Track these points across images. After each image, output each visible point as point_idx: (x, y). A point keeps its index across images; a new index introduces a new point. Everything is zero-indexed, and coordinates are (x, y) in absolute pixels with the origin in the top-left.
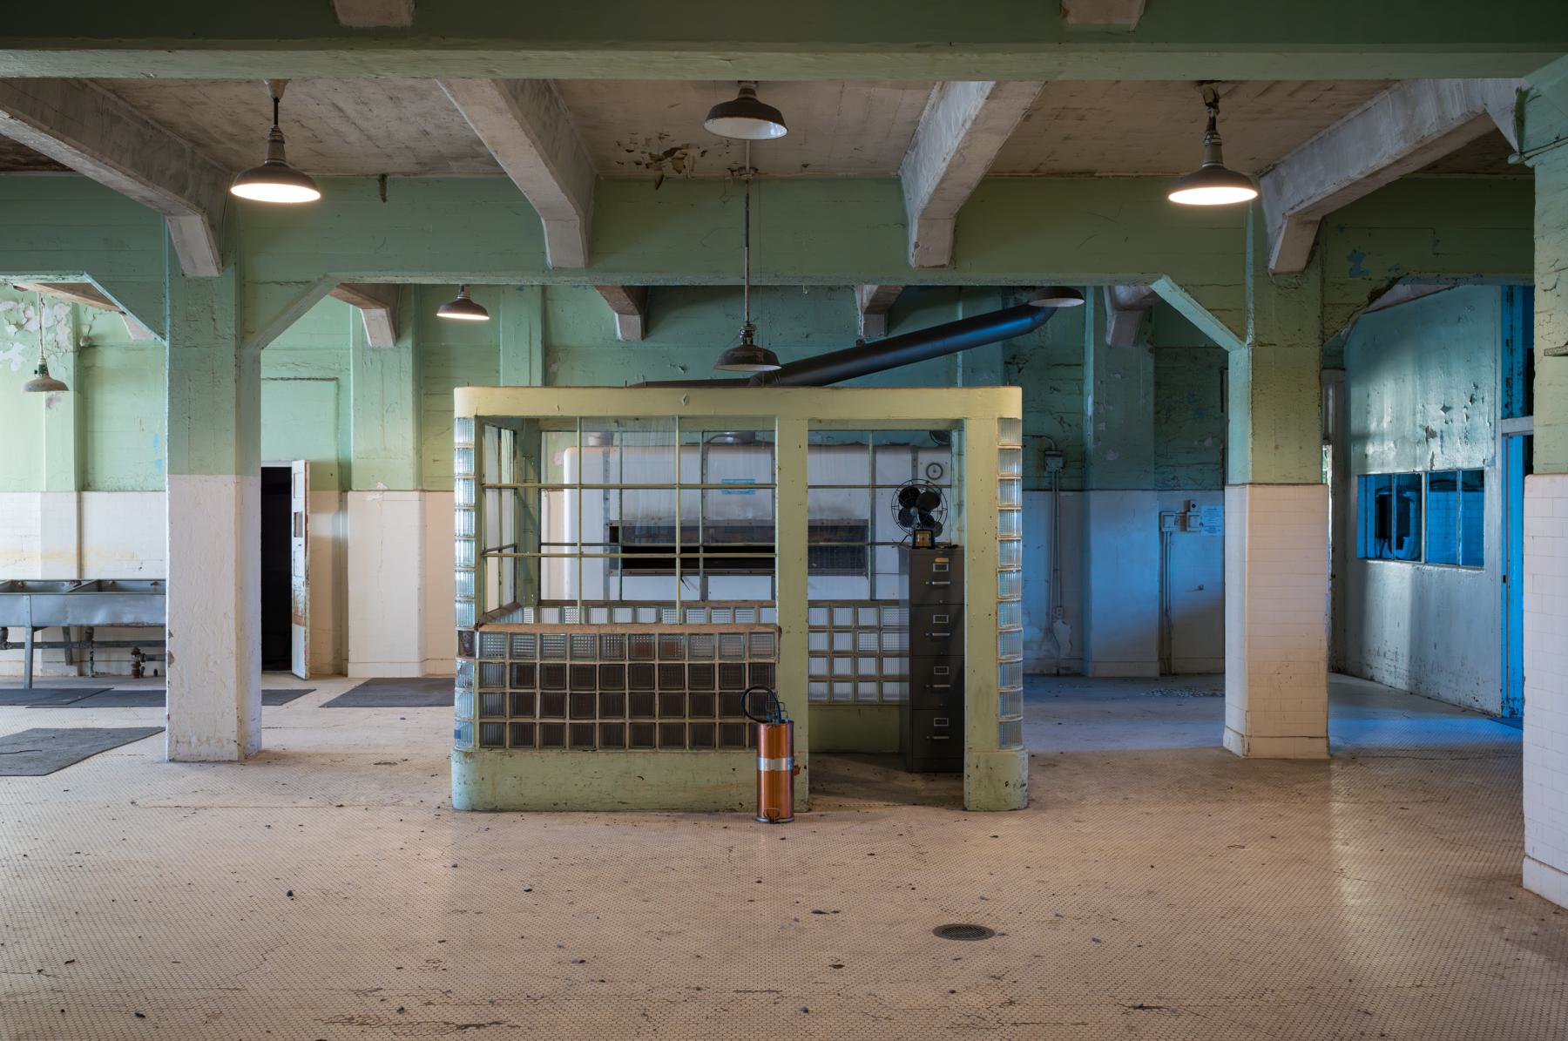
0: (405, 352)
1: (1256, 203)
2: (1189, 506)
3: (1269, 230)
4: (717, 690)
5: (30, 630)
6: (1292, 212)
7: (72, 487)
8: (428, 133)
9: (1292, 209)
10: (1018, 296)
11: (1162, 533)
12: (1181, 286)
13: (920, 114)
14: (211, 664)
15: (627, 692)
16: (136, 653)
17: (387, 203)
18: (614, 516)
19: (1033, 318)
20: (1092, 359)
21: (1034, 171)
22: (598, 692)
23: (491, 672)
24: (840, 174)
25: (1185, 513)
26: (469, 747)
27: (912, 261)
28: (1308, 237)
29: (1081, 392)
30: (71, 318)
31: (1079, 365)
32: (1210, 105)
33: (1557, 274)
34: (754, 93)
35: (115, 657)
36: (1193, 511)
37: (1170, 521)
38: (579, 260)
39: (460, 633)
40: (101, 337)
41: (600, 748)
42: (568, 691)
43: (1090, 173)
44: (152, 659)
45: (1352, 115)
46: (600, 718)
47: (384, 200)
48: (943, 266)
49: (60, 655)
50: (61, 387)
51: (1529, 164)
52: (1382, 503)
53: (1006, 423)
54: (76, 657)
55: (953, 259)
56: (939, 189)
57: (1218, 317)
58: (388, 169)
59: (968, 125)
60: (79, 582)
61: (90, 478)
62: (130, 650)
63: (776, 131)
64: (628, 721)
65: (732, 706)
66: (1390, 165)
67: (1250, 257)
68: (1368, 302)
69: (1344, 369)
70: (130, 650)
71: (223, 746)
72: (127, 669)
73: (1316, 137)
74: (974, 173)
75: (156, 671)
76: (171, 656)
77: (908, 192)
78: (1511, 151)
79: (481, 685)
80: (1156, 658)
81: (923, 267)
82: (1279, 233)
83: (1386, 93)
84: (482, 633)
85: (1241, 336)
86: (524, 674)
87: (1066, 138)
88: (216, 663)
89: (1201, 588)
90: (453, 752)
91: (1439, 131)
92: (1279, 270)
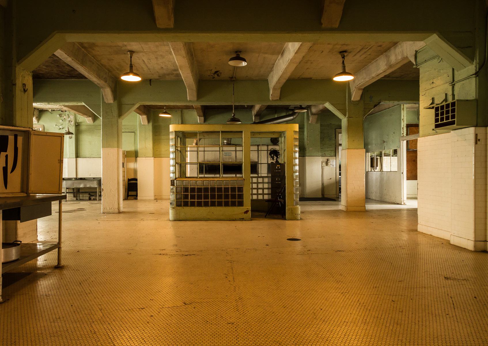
0: (150, 127)
1: (354, 81)
2: (328, 160)
3: (351, 91)
4: (230, 193)
5: (66, 189)
6: (357, 86)
7: (74, 156)
8: (163, 68)
9: (357, 85)
10: (289, 112)
11: (322, 166)
12: (331, 104)
13: (275, 62)
14: (112, 191)
15: (210, 193)
16: (89, 194)
17: (151, 86)
18: (201, 160)
19: (293, 117)
20: (306, 127)
21: (298, 78)
22: (203, 194)
23: (179, 189)
24: (254, 79)
25: (327, 162)
26: (174, 206)
27: (270, 99)
28: (360, 92)
29: (304, 134)
30: (74, 118)
31: (303, 128)
32: (343, 58)
33: (425, 91)
34: (239, 55)
35: (85, 195)
36: (329, 161)
37: (324, 164)
38: (195, 99)
39: (171, 180)
40: (81, 123)
41: (203, 206)
42: (196, 194)
43: (311, 78)
44: (93, 196)
45: (373, 61)
46: (204, 199)
47: (151, 85)
48: (278, 100)
49: (72, 195)
50: (72, 134)
53: (295, 132)
54: (76, 196)
55: (280, 98)
56: (279, 80)
57: (340, 111)
58: (151, 78)
59: (289, 61)
60: (76, 178)
61: (79, 155)
62: (88, 194)
63: (244, 64)
64: (210, 200)
65: (233, 196)
66: (383, 72)
67: (347, 97)
70: (88, 194)
71: (115, 210)
72: (88, 198)
73: (364, 68)
74: (287, 76)
75: (94, 199)
76: (103, 189)
77: (270, 82)
78: (413, 65)
79: (176, 192)
80: (321, 194)
81: (273, 100)
82: (354, 92)
83: (382, 55)
84: (177, 180)
85: (345, 115)
86: (186, 190)
87: (307, 69)
88: (113, 191)
89: (331, 179)
90: (170, 208)
92: (354, 100)
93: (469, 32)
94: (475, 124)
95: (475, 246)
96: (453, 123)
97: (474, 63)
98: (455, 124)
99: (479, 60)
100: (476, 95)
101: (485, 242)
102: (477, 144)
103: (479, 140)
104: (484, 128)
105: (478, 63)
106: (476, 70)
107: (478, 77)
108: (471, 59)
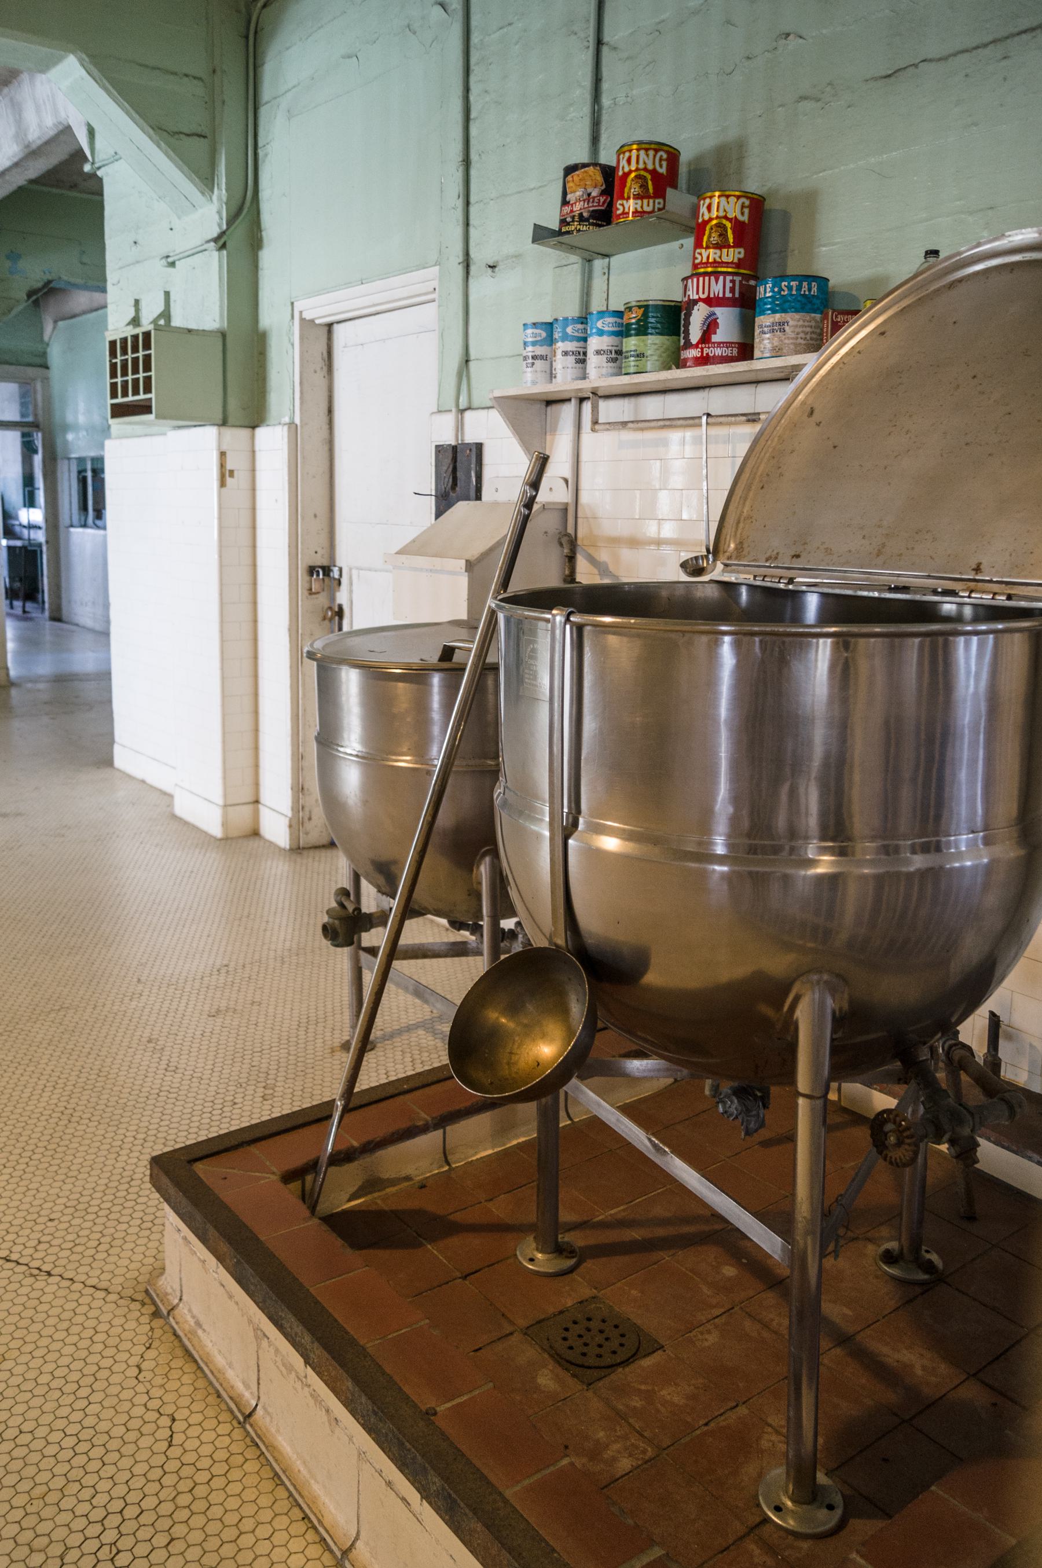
51: (99, 173)
52: (83, 481)
68: (26, 298)
69: (47, 368)
78: (86, 159)
91: (39, 138)
93: (195, 78)
94: (219, 416)
95: (225, 824)
96: (144, 408)
97: (215, 198)
98: (151, 412)
99: (227, 190)
100: (221, 315)
101: (256, 805)
102: (225, 486)
103: (231, 473)
104: (245, 433)
105: (224, 199)
106: (220, 225)
107: (225, 252)
108: (206, 180)
